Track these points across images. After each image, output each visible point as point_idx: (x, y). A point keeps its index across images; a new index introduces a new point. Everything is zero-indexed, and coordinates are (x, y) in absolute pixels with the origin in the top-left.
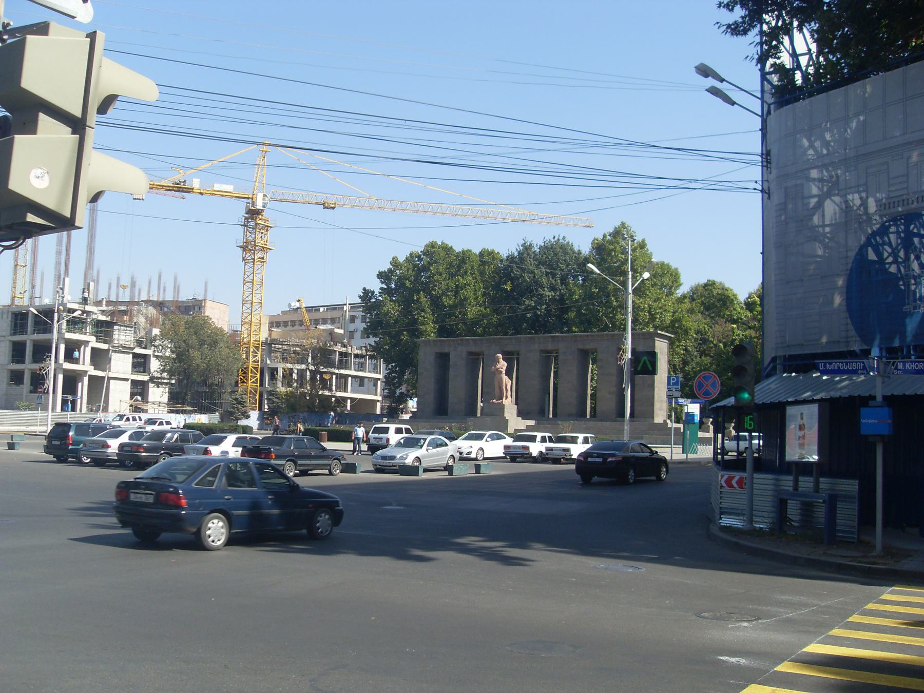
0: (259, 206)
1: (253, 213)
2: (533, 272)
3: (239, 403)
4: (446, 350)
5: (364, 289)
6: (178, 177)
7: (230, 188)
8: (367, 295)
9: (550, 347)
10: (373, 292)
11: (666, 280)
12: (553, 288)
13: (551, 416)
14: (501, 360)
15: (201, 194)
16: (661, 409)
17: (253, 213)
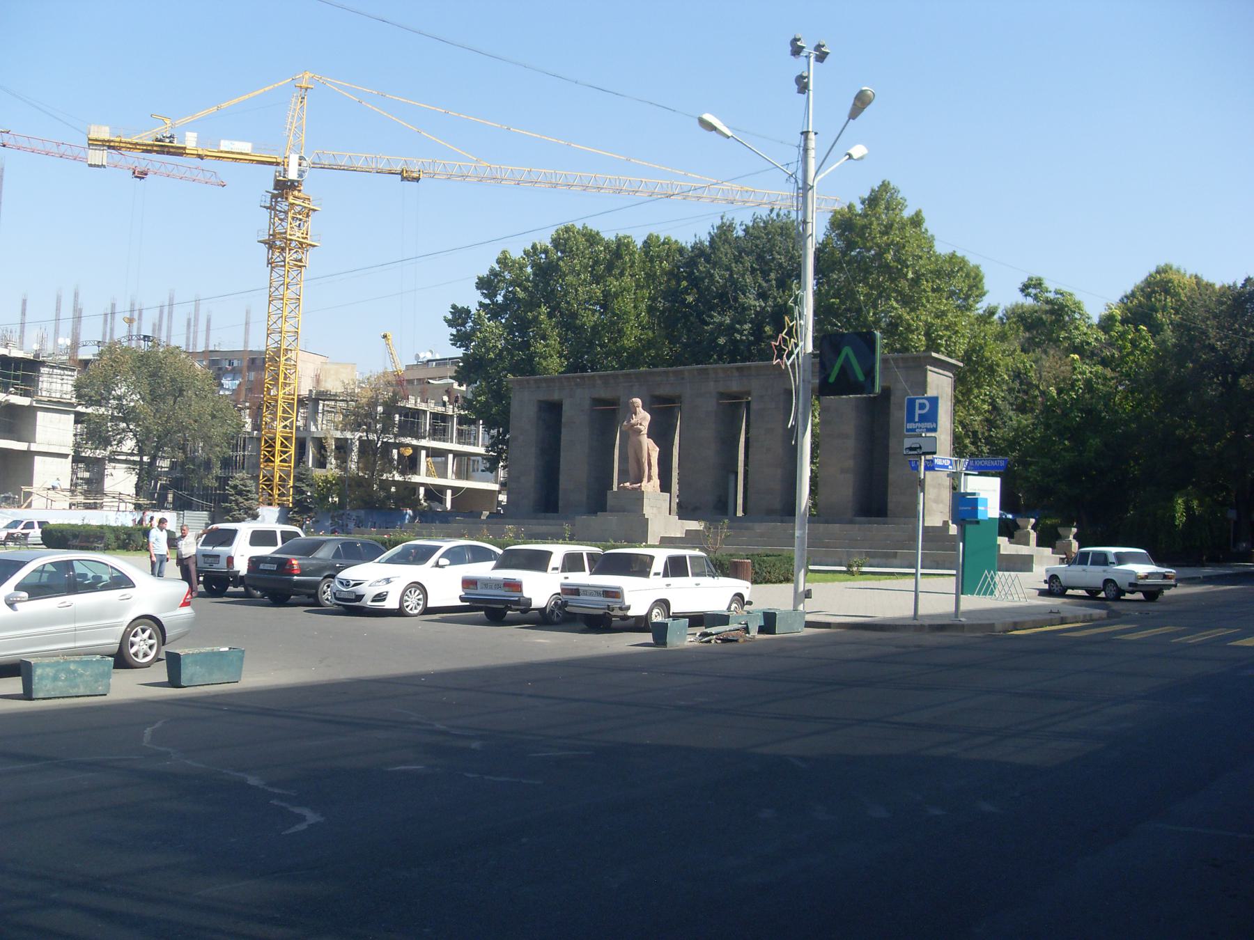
0: (293, 175)
1: (284, 187)
2: (729, 269)
3: (240, 493)
4: (556, 397)
5: (454, 307)
6: (163, 130)
7: (245, 147)
8: (459, 316)
9: (735, 387)
10: (468, 312)
11: (958, 283)
12: (762, 295)
13: (740, 513)
14: (640, 410)
15: (200, 157)
16: (937, 501)
17: (284, 187)
